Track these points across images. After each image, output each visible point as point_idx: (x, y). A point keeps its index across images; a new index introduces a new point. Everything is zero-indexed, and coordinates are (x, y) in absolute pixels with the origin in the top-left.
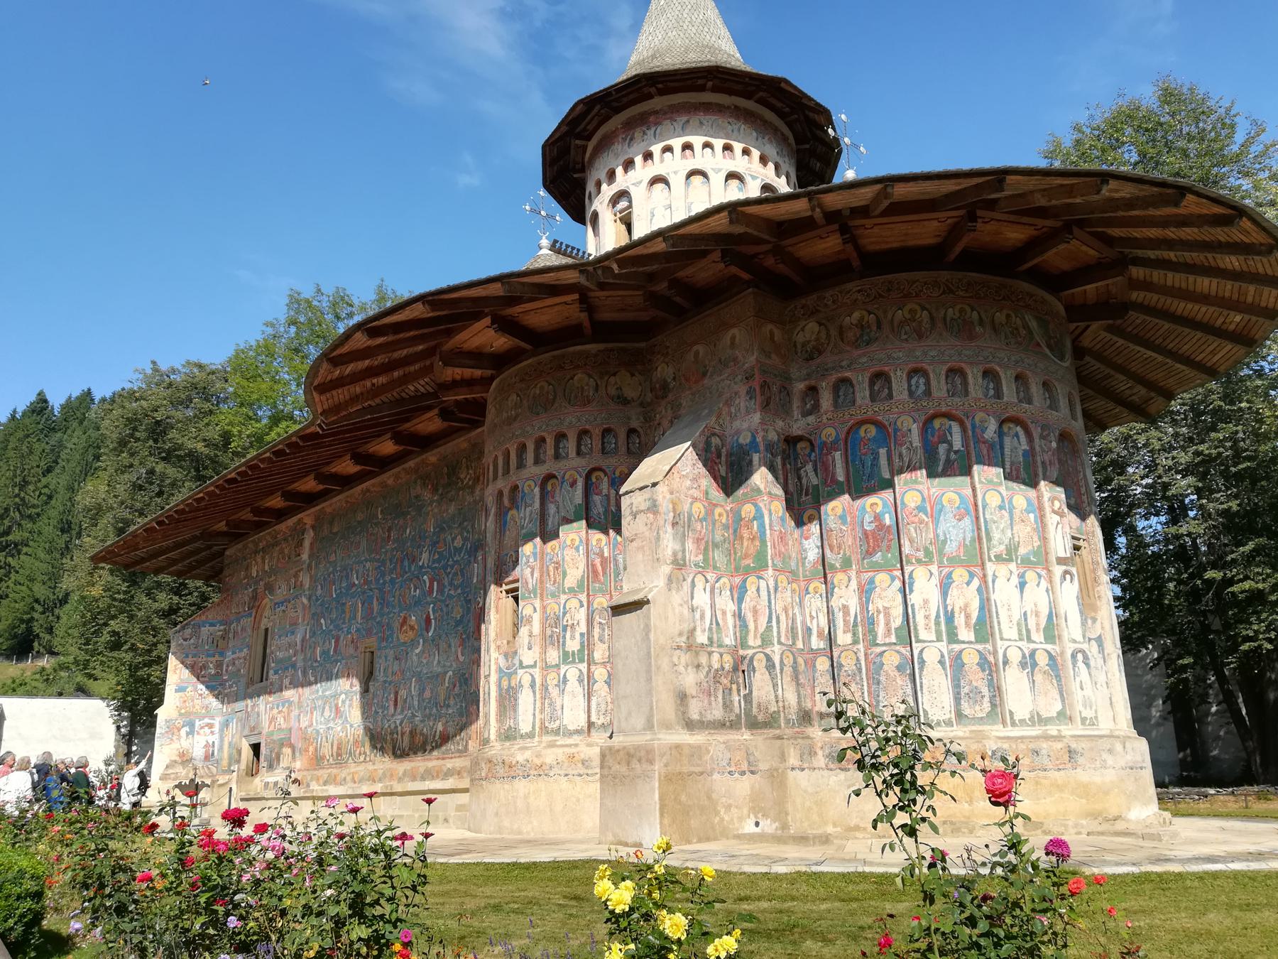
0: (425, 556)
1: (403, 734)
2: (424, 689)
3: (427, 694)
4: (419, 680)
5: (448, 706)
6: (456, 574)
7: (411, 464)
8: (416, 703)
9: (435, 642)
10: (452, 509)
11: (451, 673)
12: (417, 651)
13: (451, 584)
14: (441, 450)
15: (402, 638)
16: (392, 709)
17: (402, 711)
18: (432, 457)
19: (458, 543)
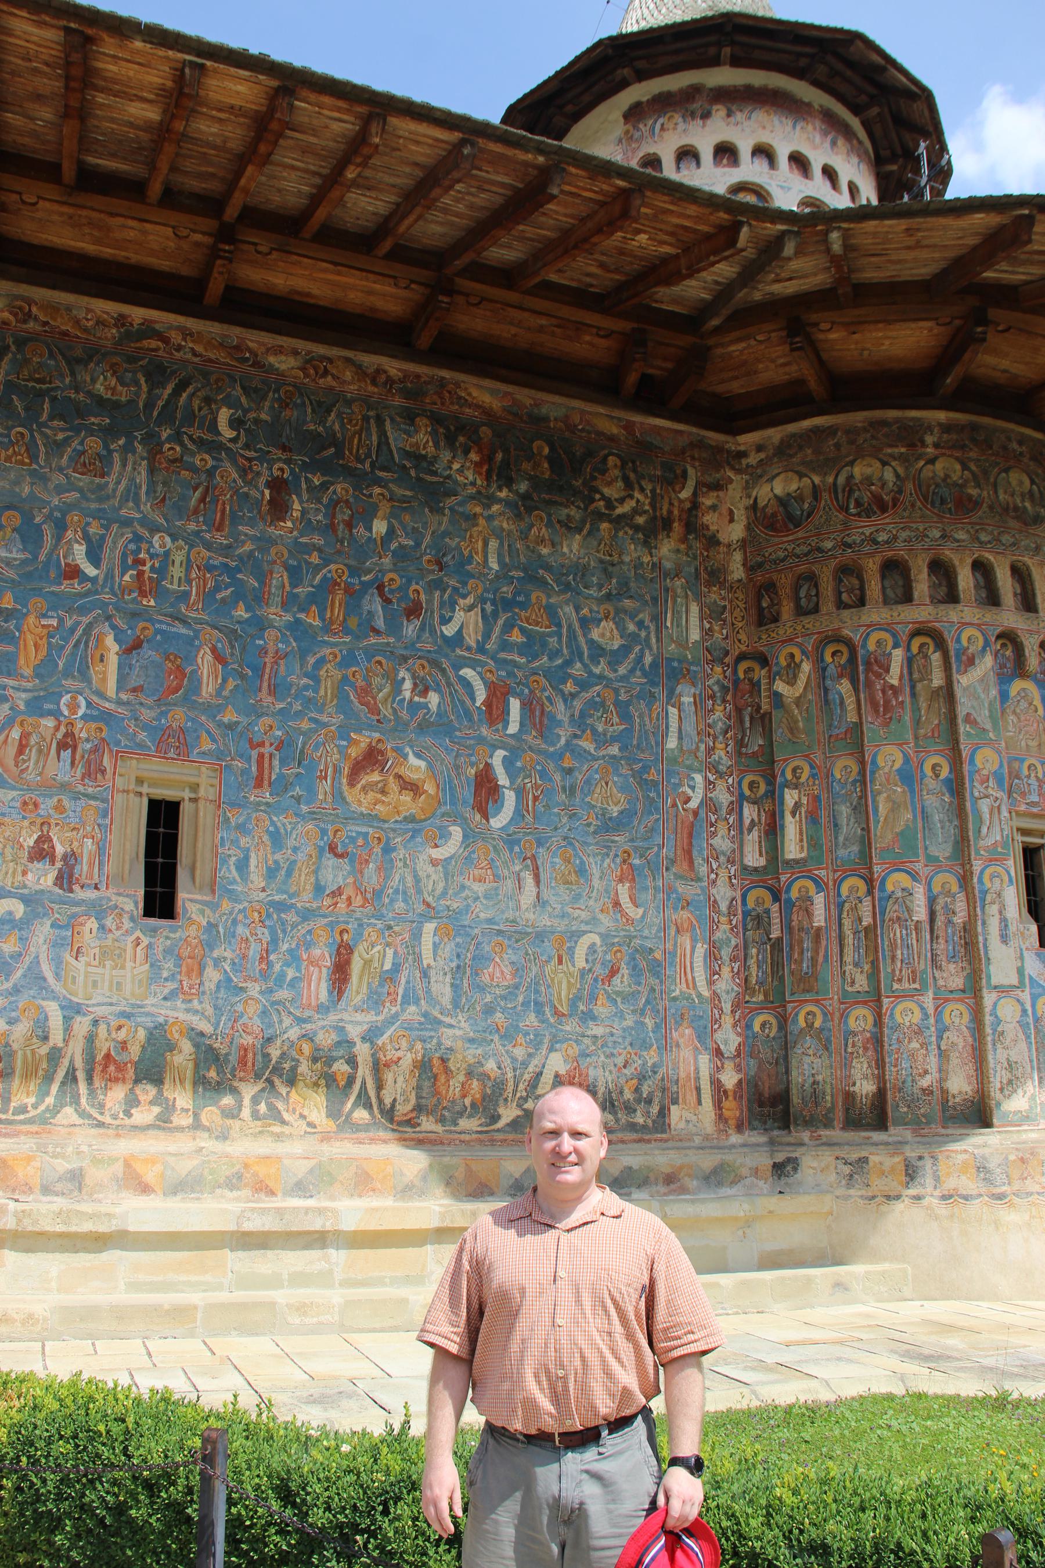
0: (464, 621)
1: (378, 1067)
2: (480, 960)
3: (499, 972)
4: (453, 925)
5: (589, 1016)
6: (592, 704)
7: (393, 367)
8: (442, 989)
9: (524, 846)
10: (573, 548)
11: (597, 939)
12: (436, 853)
13: (581, 722)
14: (525, 396)
15: (360, 801)
16: (320, 989)
17: (375, 1001)
18: (484, 394)
19: (605, 634)
